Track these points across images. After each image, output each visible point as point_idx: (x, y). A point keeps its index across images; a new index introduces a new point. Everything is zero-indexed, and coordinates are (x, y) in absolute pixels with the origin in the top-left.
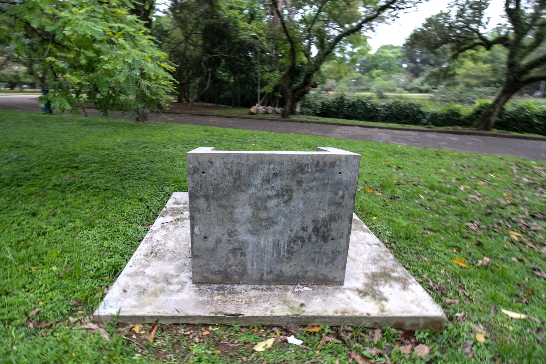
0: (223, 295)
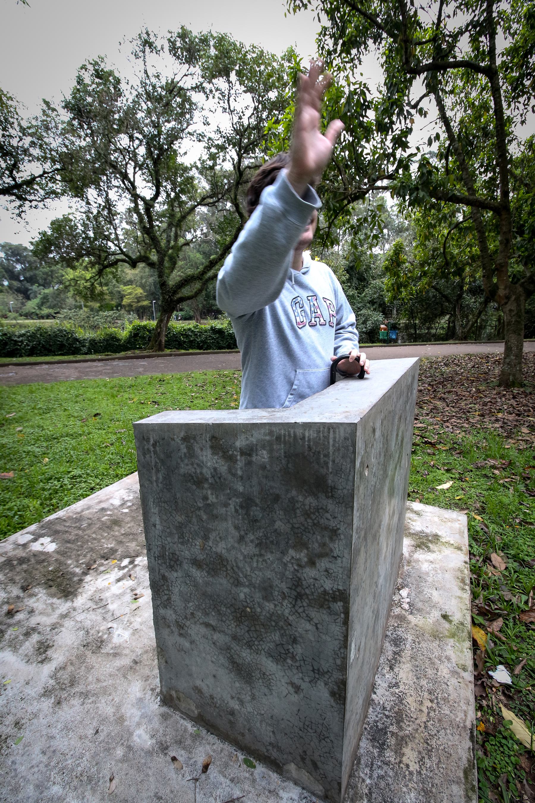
0: (402, 742)
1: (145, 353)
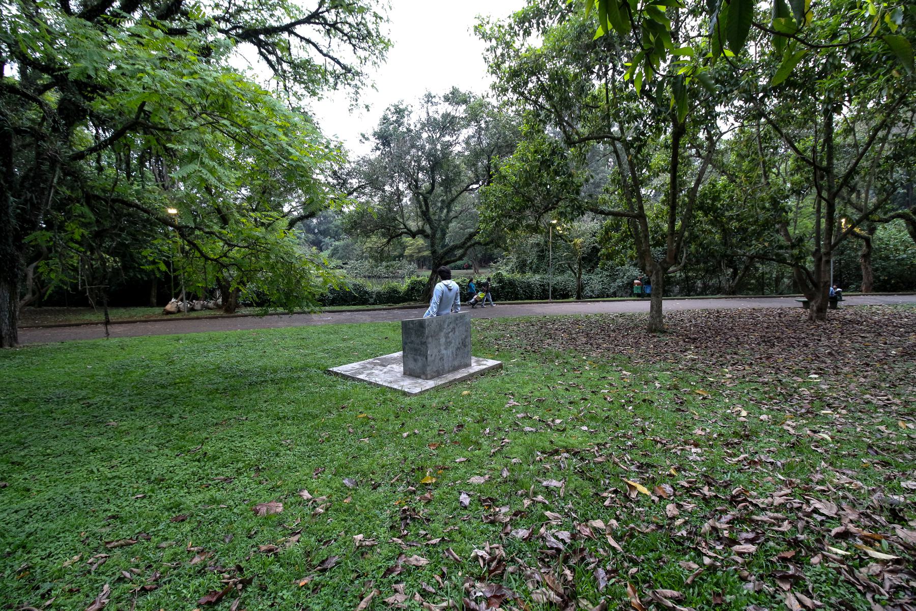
1: (418, 304)
